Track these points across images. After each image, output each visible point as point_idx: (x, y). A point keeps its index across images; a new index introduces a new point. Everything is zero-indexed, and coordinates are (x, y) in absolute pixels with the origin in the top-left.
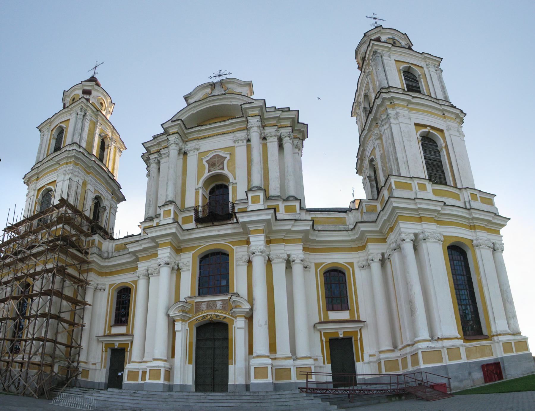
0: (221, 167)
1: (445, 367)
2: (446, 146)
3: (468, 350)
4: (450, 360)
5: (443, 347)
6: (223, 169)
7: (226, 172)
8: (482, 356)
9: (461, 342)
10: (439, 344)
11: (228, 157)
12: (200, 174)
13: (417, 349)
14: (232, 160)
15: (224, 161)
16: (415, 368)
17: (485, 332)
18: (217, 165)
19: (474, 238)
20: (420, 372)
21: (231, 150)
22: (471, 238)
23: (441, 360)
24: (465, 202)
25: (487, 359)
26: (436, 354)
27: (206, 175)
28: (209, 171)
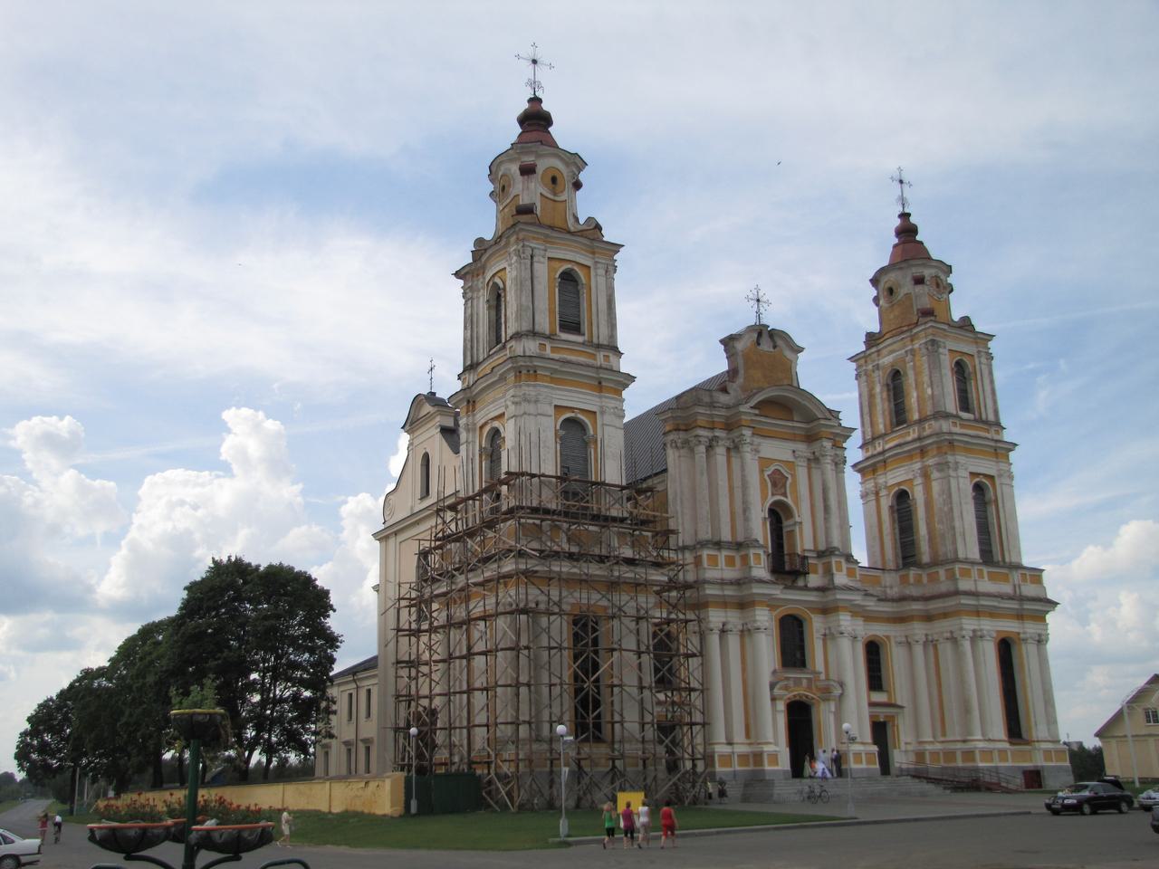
0: (783, 491)
1: (997, 767)
2: (996, 501)
3: (1013, 753)
4: (1000, 761)
5: (994, 749)
6: (785, 495)
7: (789, 501)
8: (1025, 761)
9: (1007, 745)
10: (991, 745)
11: (789, 476)
12: (764, 498)
13: (976, 748)
14: (794, 484)
15: (786, 482)
16: (969, 764)
17: (1025, 735)
18: (779, 486)
19: (1021, 631)
20: (977, 770)
21: (791, 465)
22: (1017, 630)
23: (992, 761)
24: (1015, 586)
25: (1027, 765)
26: (987, 754)
27: (771, 500)
28: (773, 495)
